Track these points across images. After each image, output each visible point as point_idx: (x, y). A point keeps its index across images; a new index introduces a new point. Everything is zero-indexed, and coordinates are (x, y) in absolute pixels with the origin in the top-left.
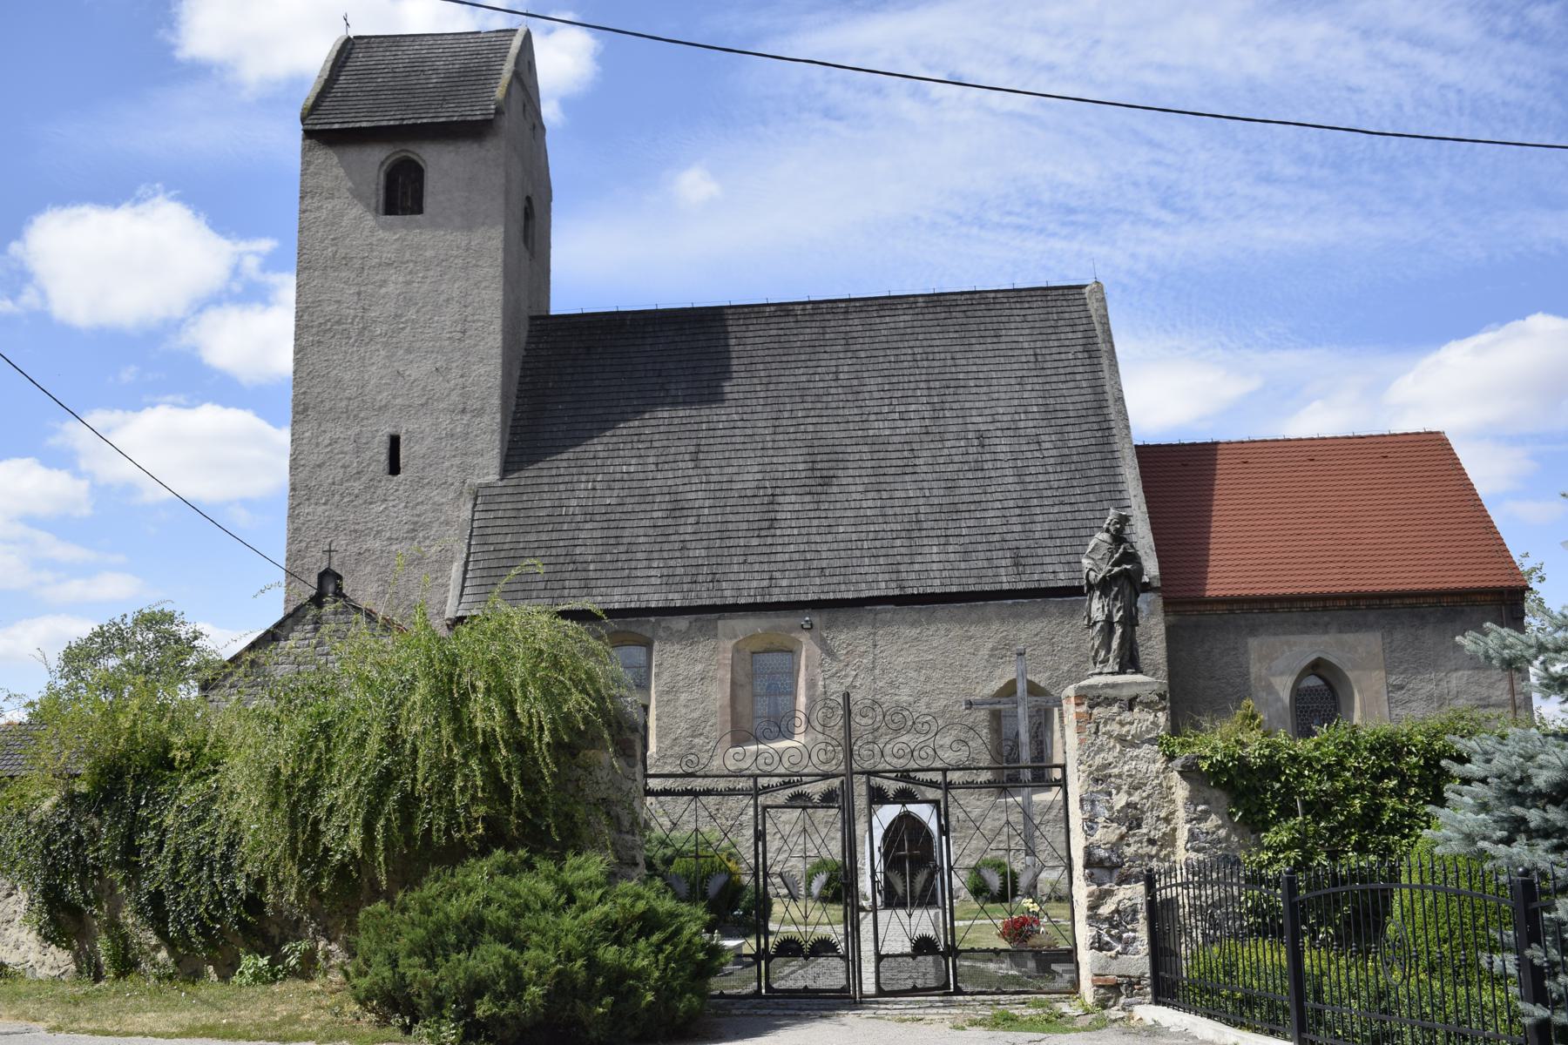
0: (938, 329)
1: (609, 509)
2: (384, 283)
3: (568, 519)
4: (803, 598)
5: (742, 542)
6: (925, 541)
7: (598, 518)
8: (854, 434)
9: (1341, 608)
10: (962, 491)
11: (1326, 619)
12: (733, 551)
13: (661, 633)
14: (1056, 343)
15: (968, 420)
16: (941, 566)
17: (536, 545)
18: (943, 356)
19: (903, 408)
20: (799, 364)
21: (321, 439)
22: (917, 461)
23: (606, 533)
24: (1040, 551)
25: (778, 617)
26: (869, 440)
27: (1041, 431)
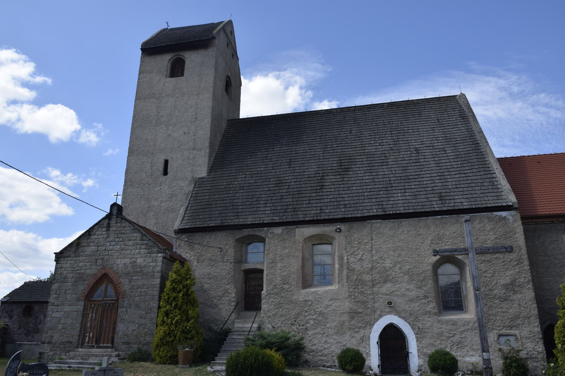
0: (394, 114)
1: (251, 185)
3: (233, 189)
4: (336, 217)
5: (308, 195)
6: (395, 192)
7: (245, 188)
8: (359, 152)
10: (411, 171)
12: (304, 199)
13: (269, 235)
14: (447, 115)
15: (410, 144)
16: (403, 202)
17: (217, 199)
18: (396, 122)
19: (380, 141)
20: (335, 129)
22: (388, 161)
23: (248, 194)
24: (452, 194)
25: (324, 226)
26: (366, 154)
27: (445, 146)
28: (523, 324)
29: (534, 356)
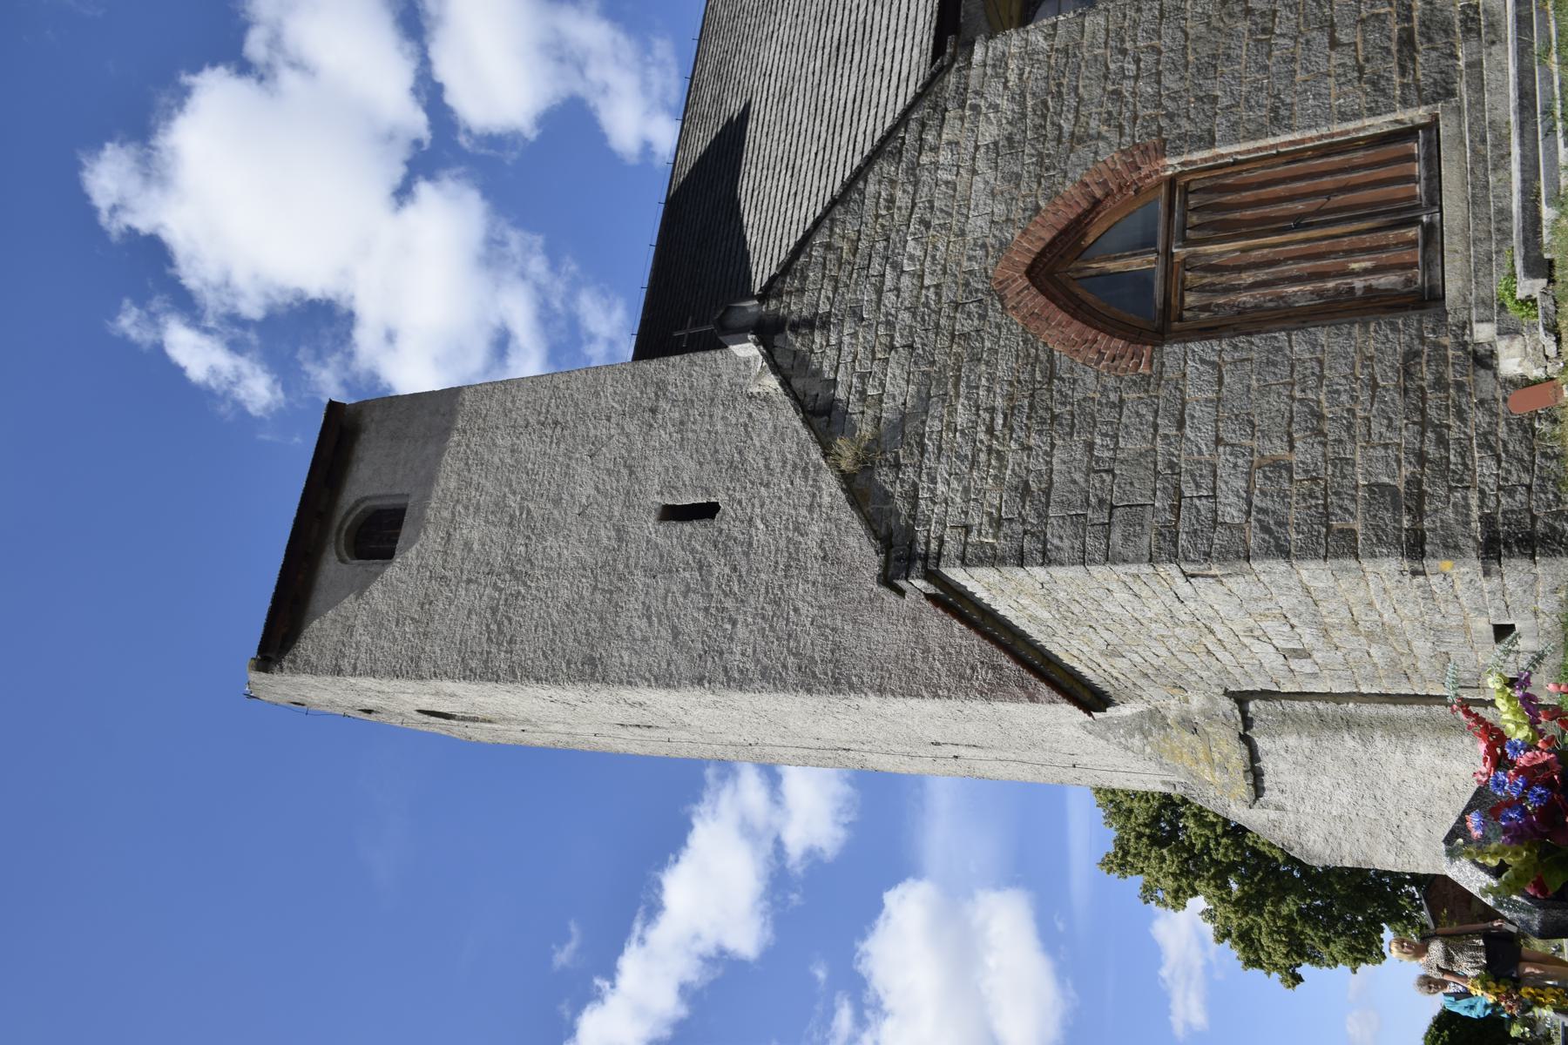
2: (468, 546)
21: (638, 635)
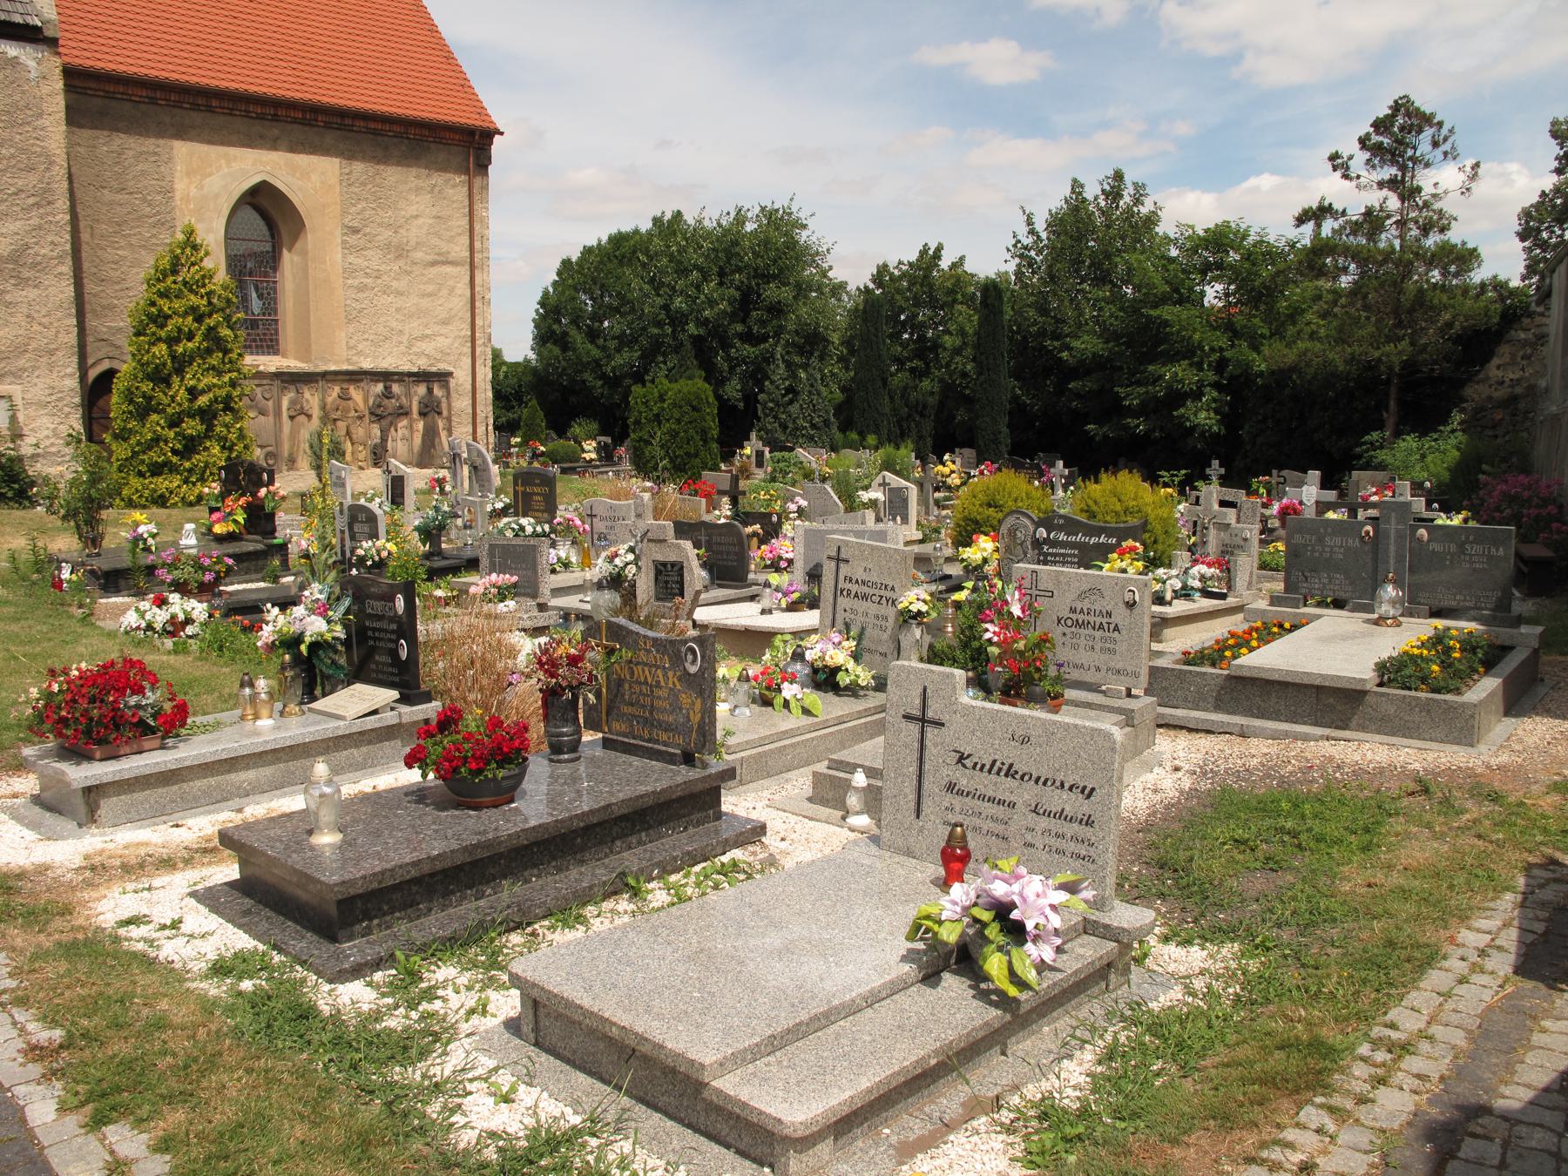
9: (295, 121)
11: (276, 132)
28: (34, 368)
29: (53, 450)
